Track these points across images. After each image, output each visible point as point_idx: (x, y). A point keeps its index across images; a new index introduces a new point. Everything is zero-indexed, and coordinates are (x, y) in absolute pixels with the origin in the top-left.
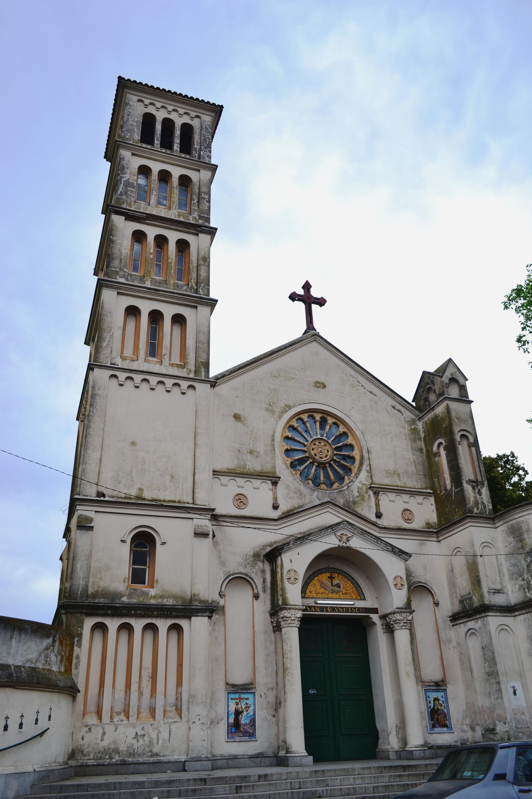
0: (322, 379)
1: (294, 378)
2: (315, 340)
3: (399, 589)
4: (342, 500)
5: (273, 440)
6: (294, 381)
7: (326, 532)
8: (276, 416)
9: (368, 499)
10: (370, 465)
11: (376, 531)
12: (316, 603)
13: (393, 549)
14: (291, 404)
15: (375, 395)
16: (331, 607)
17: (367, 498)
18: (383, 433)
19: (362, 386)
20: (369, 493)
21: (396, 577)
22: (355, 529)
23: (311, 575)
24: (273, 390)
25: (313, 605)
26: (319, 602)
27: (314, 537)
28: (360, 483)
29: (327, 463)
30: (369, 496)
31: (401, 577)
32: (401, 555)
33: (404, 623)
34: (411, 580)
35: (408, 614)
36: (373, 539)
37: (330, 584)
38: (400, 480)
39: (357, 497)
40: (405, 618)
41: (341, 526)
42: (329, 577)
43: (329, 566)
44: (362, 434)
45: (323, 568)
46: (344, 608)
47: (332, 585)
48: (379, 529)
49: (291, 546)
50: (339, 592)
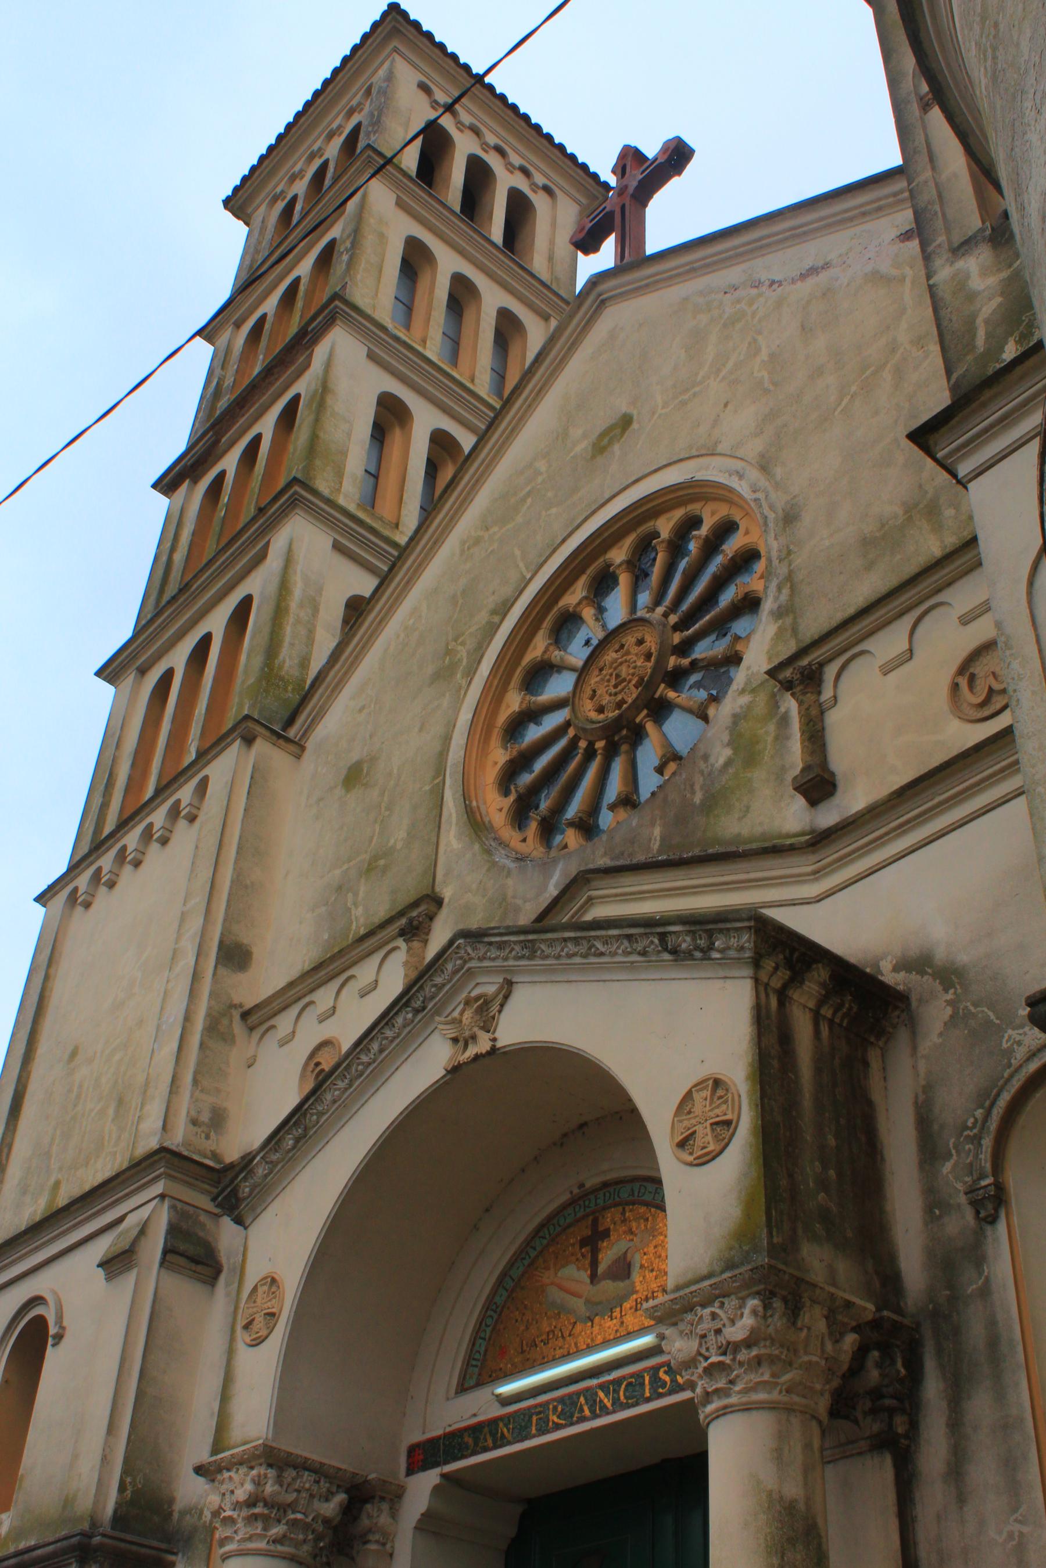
0: (623, 406)
1: (529, 494)
2: (603, 302)
3: (706, 1159)
4: (657, 831)
5: (440, 770)
6: (529, 500)
7: (389, 1033)
8: (459, 676)
9: (777, 738)
10: (790, 578)
11: (798, 879)
12: (505, 1401)
13: (662, 937)
14: (507, 591)
15: (826, 266)
16: (561, 1400)
17: (770, 739)
18: (854, 388)
19: (773, 283)
20: (782, 710)
21: (688, 1096)
22: (501, 946)
23: (511, 1264)
24: (464, 592)
25: (498, 1411)
26: (507, 1389)
27: (341, 1085)
28: (743, 692)
29: (636, 707)
30: (784, 721)
31: (717, 1083)
32: (711, 947)
33: (709, 1371)
34: (1010, 1052)
35: (731, 1303)
36: (571, 948)
37: (584, 1276)
38: (938, 527)
39: (728, 763)
40: (711, 1337)
41: (450, 967)
42: (584, 1242)
43: (582, 1186)
44: (764, 466)
45: (564, 1207)
46: (617, 1382)
47: (594, 1277)
48: (813, 858)
49: (260, 1171)
50: (620, 1301)
